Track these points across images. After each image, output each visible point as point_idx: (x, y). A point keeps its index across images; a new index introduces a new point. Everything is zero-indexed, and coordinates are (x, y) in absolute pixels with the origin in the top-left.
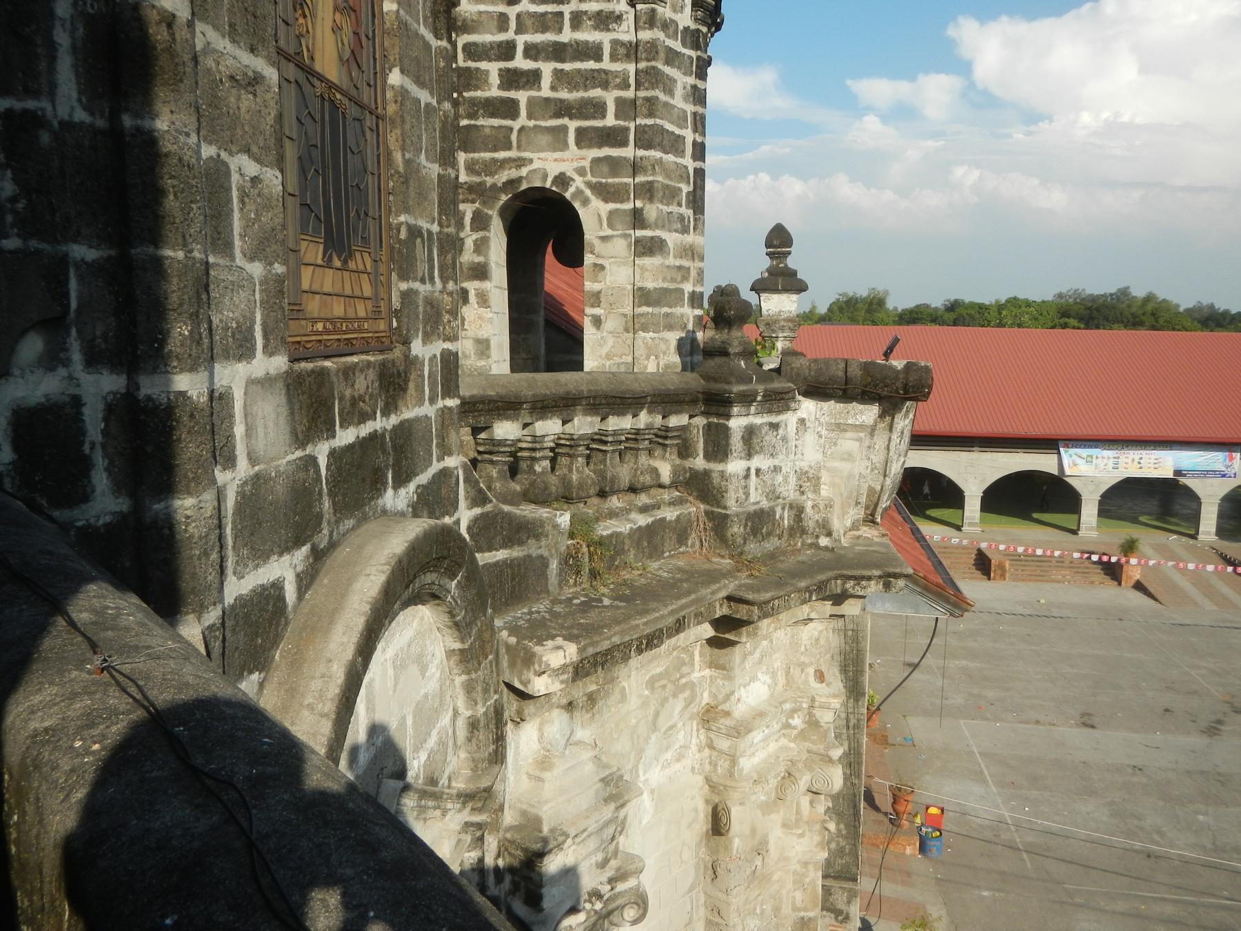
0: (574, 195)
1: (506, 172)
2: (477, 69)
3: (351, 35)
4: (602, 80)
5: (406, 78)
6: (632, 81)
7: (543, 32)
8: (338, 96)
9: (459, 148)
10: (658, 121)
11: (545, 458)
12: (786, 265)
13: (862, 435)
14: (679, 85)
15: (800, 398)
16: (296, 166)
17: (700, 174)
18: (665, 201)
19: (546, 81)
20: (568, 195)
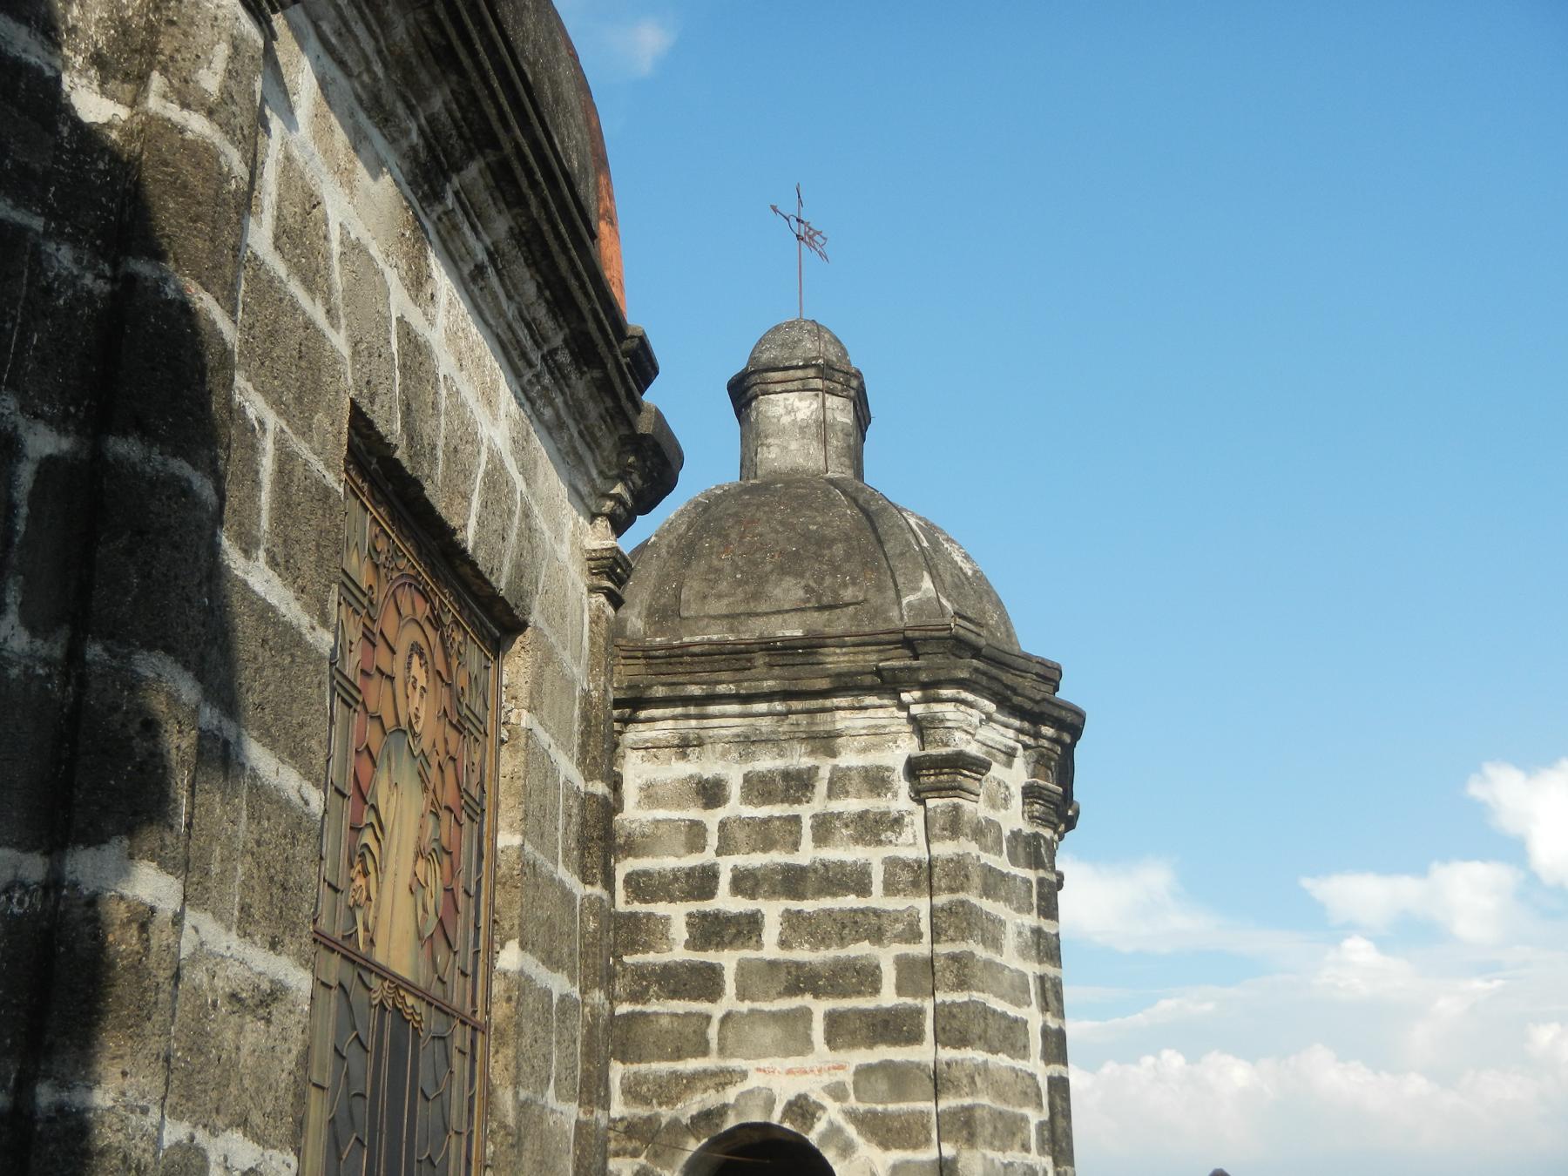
0: (826, 1137)
1: (698, 1097)
2: (649, 915)
3: (441, 893)
4: (872, 927)
5: (528, 956)
6: (925, 926)
7: (766, 849)
8: (410, 1000)
9: (613, 1054)
14: (1010, 930)
16: (324, 1132)
17: (1060, 1087)
18: (997, 1143)
19: (772, 931)
20: (813, 1137)
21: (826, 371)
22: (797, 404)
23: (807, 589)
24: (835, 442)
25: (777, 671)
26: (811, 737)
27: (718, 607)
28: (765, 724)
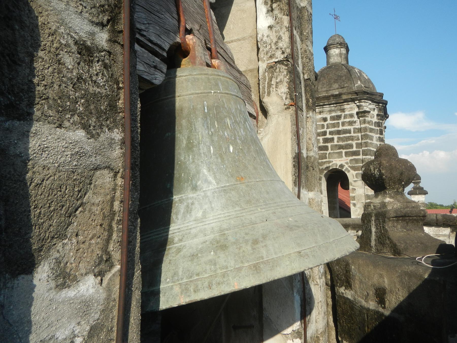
0: (345, 170)
4: (352, 138)
6: (360, 138)
7: (334, 128)
10: (369, 148)
12: (419, 186)
14: (375, 137)
19: (336, 140)
20: (343, 170)
21: (341, 44)
22: (336, 51)
23: (339, 85)
24: (343, 57)
25: (334, 100)
26: (341, 110)
27: (325, 89)
28: (333, 108)
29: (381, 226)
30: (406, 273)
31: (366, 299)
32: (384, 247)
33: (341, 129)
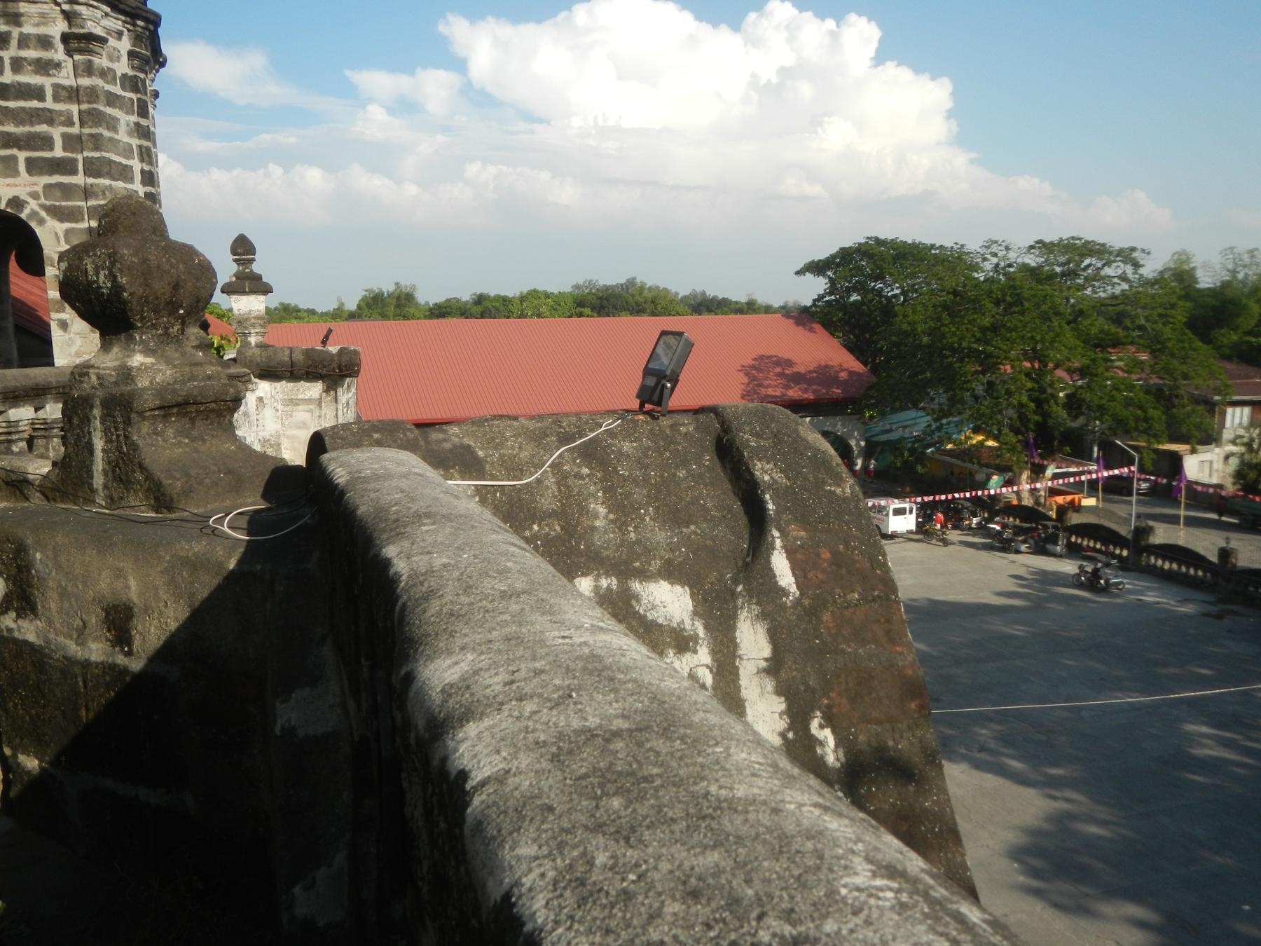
0: (30, 216)
4: (49, 117)
6: (76, 119)
10: (104, 154)
11: (22, 440)
12: (252, 270)
13: (312, 407)
14: (122, 121)
15: (256, 380)
20: (23, 216)
29: (121, 433)
30: (186, 562)
31: (79, 637)
32: (128, 491)
33: (8, 81)
